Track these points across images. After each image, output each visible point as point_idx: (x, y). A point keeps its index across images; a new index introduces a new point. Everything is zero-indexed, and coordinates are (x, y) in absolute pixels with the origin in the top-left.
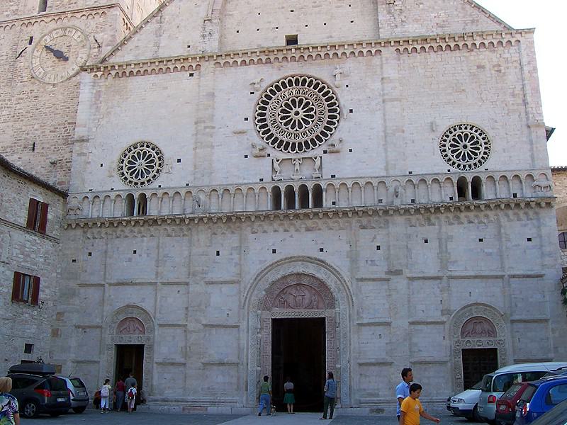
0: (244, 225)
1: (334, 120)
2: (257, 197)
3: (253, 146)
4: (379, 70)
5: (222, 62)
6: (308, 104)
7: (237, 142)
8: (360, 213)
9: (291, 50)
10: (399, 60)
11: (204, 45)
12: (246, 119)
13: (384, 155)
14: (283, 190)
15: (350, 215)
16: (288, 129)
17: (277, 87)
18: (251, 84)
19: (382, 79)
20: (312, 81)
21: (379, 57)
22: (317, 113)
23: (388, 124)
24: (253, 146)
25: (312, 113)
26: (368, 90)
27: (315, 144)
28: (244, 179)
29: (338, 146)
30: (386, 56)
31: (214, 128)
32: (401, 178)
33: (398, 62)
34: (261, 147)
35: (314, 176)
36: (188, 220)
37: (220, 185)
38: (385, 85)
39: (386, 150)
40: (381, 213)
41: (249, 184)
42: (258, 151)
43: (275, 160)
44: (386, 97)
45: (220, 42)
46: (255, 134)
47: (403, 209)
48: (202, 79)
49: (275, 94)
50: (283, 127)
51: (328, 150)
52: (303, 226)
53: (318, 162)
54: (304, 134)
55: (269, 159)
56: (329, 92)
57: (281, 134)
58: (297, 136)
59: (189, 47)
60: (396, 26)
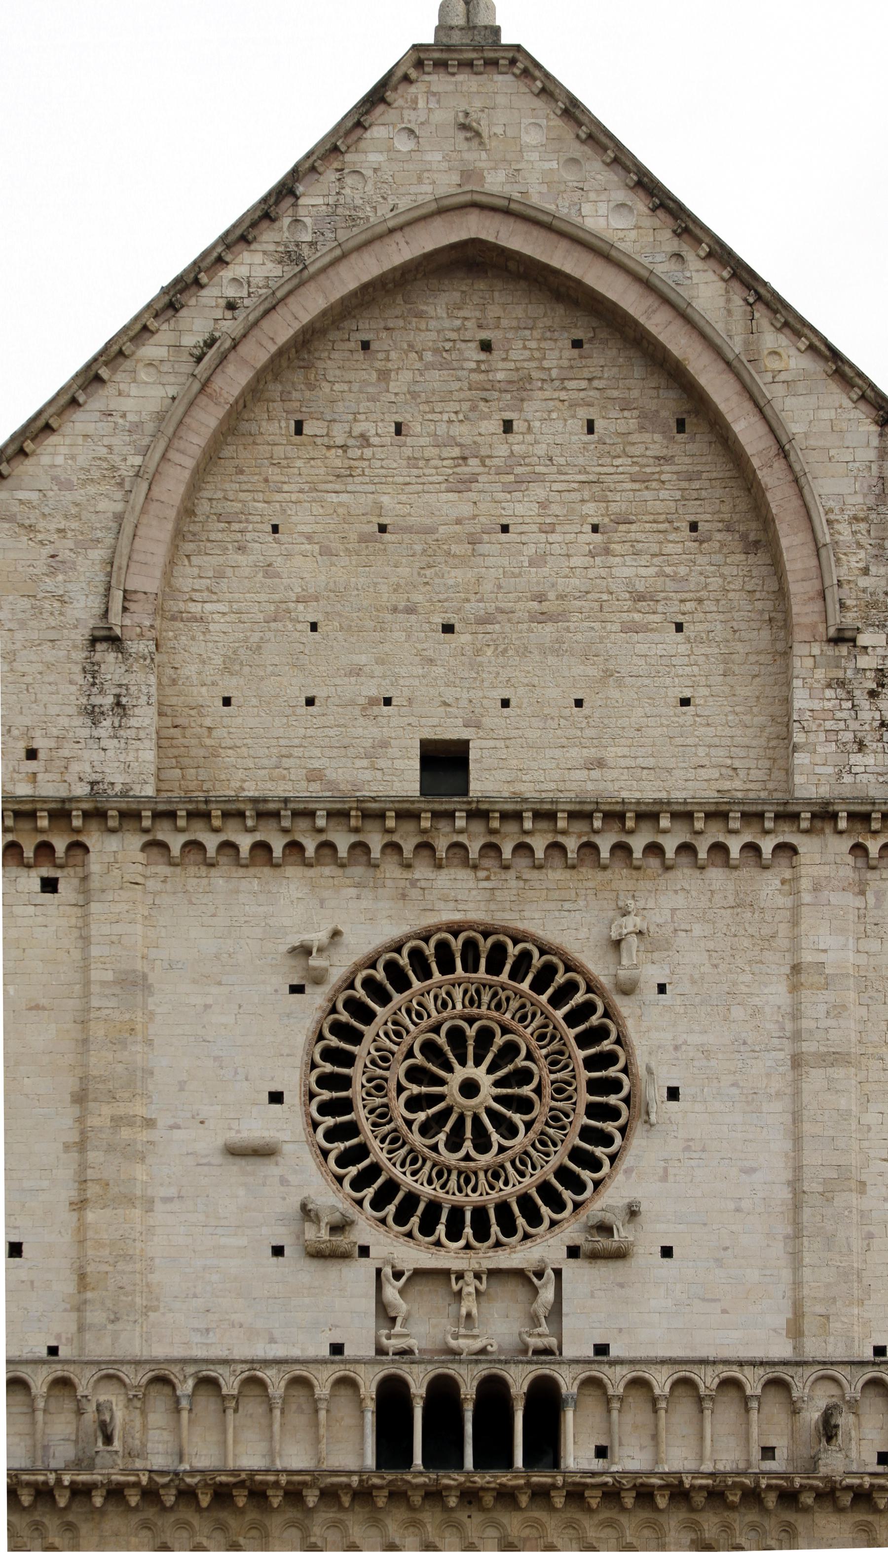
0: (275, 1522)
1: (610, 1127)
2: (322, 1414)
3: (307, 1212)
4: (784, 929)
5: (176, 842)
6: (510, 1051)
7: (241, 1192)
8: (699, 1499)
9: (450, 815)
10: (862, 893)
11: (97, 755)
12: (276, 1098)
13: (786, 1275)
14: (418, 1388)
15: (662, 1502)
16: (434, 1148)
17: (392, 968)
18: (293, 951)
19: (796, 969)
20: (525, 957)
21: (787, 874)
22: (548, 1090)
23: (811, 1157)
24: (307, 1212)
25: (527, 1090)
26: (737, 1012)
27: (534, 1219)
28: (272, 1340)
29: (623, 1234)
30: (816, 871)
31: (150, 1123)
32: (847, 1369)
33: (859, 902)
34: (336, 1217)
35: (534, 1342)
36: (67, 1493)
37: (185, 1361)
38: (805, 993)
39: (796, 1260)
40: (771, 1501)
41: (297, 1361)
42: (324, 1234)
43: (388, 1271)
44: (808, 1047)
45: (162, 743)
46: (309, 1161)
47: (849, 1488)
48: (94, 907)
49: (384, 999)
50: (416, 1139)
51: (586, 1247)
52: (492, 1532)
53: (547, 1294)
54: (496, 1176)
55: (364, 1269)
56: (588, 1008)
57: (408, 1169)
58: (467, 1181)
59: (32, 754)
60: (861, 746)
